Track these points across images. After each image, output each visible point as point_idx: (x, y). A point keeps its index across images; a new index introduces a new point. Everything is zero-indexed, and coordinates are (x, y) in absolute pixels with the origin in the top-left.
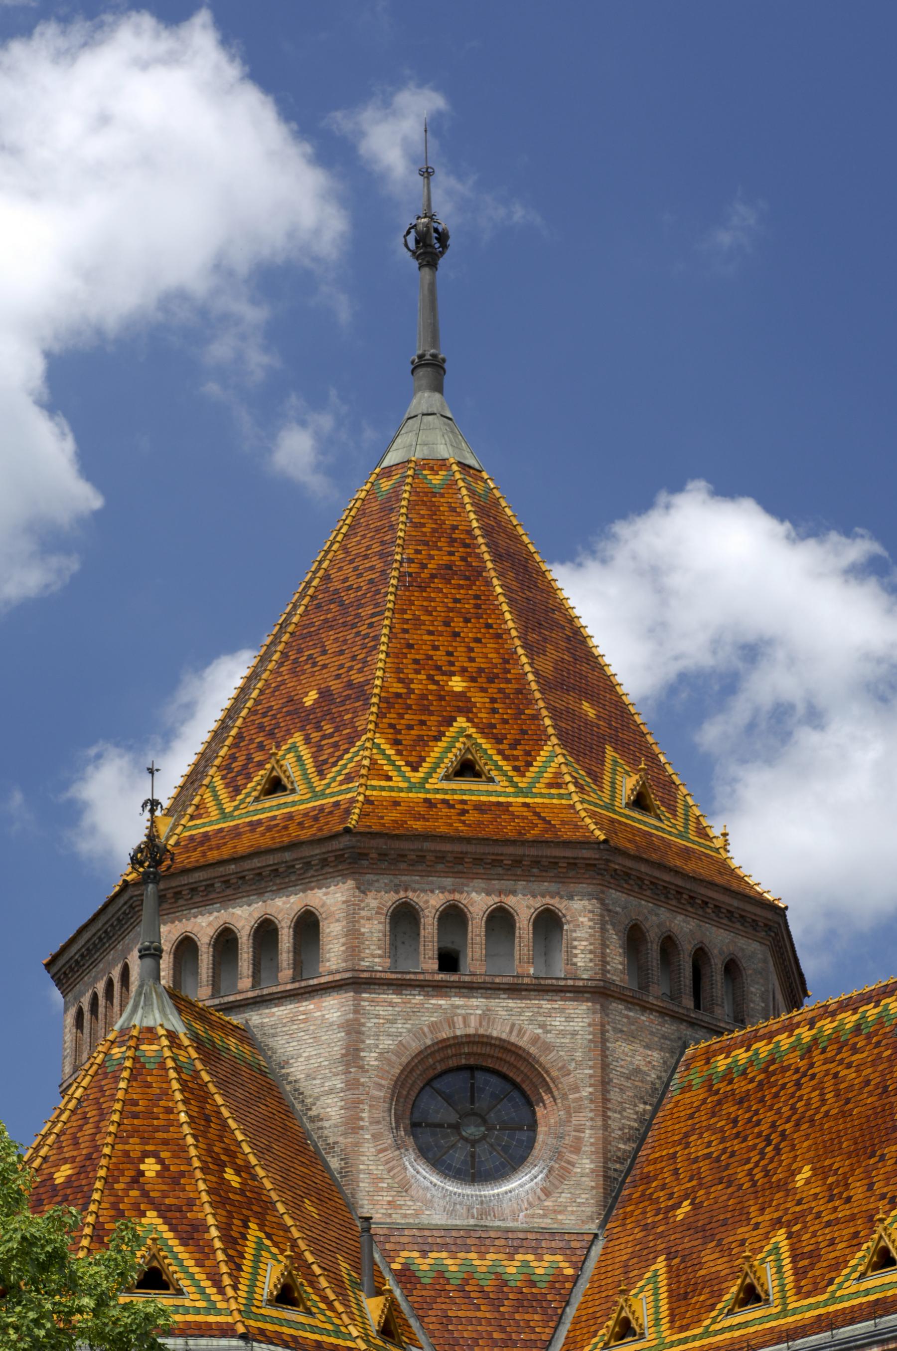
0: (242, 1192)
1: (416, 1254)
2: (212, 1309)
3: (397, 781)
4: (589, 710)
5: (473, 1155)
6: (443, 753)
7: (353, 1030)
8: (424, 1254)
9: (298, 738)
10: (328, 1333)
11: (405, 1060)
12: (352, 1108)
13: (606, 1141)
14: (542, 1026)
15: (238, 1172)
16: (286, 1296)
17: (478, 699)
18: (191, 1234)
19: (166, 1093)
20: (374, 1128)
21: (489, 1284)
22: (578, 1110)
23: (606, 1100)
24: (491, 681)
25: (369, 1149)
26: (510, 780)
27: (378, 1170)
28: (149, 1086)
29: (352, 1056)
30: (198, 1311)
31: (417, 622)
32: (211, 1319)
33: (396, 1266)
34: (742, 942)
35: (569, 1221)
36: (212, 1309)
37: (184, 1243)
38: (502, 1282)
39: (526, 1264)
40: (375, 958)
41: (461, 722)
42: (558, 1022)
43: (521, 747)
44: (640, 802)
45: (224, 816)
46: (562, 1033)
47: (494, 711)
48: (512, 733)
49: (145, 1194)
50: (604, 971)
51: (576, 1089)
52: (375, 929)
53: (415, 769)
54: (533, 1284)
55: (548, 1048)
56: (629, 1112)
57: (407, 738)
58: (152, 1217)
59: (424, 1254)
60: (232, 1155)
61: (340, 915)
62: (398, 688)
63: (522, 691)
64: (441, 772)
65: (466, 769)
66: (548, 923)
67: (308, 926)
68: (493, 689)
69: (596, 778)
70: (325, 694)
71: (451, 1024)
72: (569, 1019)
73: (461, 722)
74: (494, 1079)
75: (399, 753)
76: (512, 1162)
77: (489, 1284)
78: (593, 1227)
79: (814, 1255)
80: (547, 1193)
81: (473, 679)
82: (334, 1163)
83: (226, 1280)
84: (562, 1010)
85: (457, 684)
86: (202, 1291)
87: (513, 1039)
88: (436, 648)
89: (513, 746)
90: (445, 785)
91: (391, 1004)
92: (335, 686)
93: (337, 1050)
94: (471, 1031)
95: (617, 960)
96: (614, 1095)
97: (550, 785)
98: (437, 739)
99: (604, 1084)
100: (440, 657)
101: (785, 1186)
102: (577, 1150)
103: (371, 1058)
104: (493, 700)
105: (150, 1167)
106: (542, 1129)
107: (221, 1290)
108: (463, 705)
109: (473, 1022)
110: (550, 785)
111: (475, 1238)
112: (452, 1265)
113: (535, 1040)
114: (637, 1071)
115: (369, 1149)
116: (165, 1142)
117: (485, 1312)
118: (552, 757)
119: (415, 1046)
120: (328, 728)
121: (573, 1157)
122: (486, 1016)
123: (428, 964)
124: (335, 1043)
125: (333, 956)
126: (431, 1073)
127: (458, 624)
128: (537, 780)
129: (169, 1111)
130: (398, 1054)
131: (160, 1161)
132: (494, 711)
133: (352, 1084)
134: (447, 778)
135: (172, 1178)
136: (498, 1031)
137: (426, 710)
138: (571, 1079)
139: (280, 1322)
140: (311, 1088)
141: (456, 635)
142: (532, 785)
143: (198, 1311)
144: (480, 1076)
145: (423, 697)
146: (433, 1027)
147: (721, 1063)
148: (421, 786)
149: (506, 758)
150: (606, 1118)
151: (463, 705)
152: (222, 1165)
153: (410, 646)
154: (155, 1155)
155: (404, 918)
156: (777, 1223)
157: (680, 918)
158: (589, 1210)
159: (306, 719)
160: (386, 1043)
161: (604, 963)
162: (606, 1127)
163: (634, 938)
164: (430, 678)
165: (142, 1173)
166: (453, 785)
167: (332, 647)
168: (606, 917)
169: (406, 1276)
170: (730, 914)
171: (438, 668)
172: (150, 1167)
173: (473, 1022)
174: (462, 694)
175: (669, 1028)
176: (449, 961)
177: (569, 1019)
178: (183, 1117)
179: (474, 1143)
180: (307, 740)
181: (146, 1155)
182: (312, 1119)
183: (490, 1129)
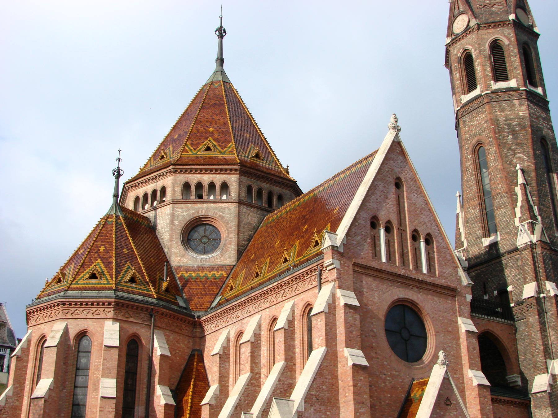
0: (127, 254)
1: (184, 273)
2: (109, 283)
3: (190, 153)
4: (247, 135)
5: (204, 247)
6: (203, 146)
7: (173, 215)
8: (187, 272)
9: (171, 146)
10: (144, 290)
11: (185, 222)
12: (171, 236)
13: (238, 241)
14: (222, 212)
15: (127, 250)
16: (132, 280)
17: (216, 133)
18: (108, 264)
19: (112, 230)
20: (176, 240)
21: (203, 280)
22: (231, 233)
23: (239, 230)
24: (220, 128)
25: (174, 246)
26: (220, 152)
27: (177, 251)
28: (107, 228)
29: (172, 222)
30: (104, 284)
31: (204, 117)
32: (107, 286)
33: (179, 276)
34: (284, 190)
35: (227, 263)
36: (109, 283)
37: (106, 267)
38: (207, 278)
39: (214, 274)
40: (179, 197)
41: (210, 138)
42: (226, 211)
43: (224, 143)
44: (257, 156)
45: (151, 166)
46: (227, 214)
47: (219, 135)
48: (223, 140)
49: (99, 255)
50: (239, 197)
51: (230, 228)
52: (179, 189)
53: (195, 150)
54: (215, 279)
55: (223, 217)
56: (246, 234)
57: (195, 143)
58: (99, 261)
59: (187, 272)
60: (127, 245)
61: (170, 186)
62: (196, 132)
63: (228, 131)
64: (202, 150)
65: (208, 149)
66: (225, 186)
67: (163, 190)
68: (220, 131)
69: (245, 151)
70: (179, 135)
71: (198, 213)
72: (229, 210)
73: (210, 138)
74: (211, 227)
75: (192, 146)
76: (215, 248)
77: (203, 280)
78: (234, 264)
79: (273, 263)
80: (222, 256)
81: (215, 129)
82: (166, 250)
83: (114, 276)
84: (228, 207)
85: (211, 130)
86: (107, 279)
87: (214, 215)
88: (207, 122)
89: (222, 143)
90: (202, 153)
91: (182, 208)
92: (182, 133)
93: (168, 221)
94: (203, 214)
95: (244, 194)
96: (242, 229)
97: (230, 152)
98: (203, 142)
99: (239, 226)
100: (208, 124)
101: (273, 247)
102: (230, 244)
103: (176, 222)
104: (219, 133)
105: (102, 249)
106: (222, 239)
107: (112, 278)
108: (212, 135)
109: (204, 212)
110: (230, 152)
111: (201, 268)
112: (194, 275)
113: (220, 216)
114: (249, 223)
115: (174, 246)
116: (108, 242)
117: (201, 287)
118: (232, 145)
119: (188, 219)
120: (177, 142)
121: (229, 246)
122: (208, 210)
123: (193, 197)
124: (168, 218)
125: (168, 197)
126: (194, 226)
127: (214, 116)
128: (227, 151)
129: (111, 234)
130: (183, 221)
131: (105, 247)
132: (219, 135)
133: (171, 229)
134: (203, 151)
135: (106, 251)
136: (210, 214)
137: (202, 136)
138: (229, 225)
139: (128, 287)
140: (162, 231)
141: (213, 119)
142: (225, 152)
143: (104, 284)
144: (207, 226)
145: (202, 133)
146: (193, 213)
147: (271, 219)
148: (196, 154)
149: (220, 146)
150: (238, 235)
151: (212, 135)
152: (123, 248)
153: (201, 122)
154: (104, 245)
155: (186, 186)
156: (269, 256)
157: (264, 184)
158: (233, 260)
159: (174, 141)
160: (181, 218)
161: (239, 195)
162: (238, 237)
163: (249, 190)
164: (205, 129)
165: (99, 250)
166: (204, 153)
167: (184, 124)
168: (240, 183)
169: (181, 278)
170: (279, 183)
171: (207, 126)
172: (102, 249)
173: (204, 212)
174: (212, 133)
175: (260, 212)
176: (200, 197)
177: (229, 210)
178: (114, 236)
179: (205, 244)
180: (172, 147)
181: (102, 245)
182: (162, 239)
183: (209, 240)
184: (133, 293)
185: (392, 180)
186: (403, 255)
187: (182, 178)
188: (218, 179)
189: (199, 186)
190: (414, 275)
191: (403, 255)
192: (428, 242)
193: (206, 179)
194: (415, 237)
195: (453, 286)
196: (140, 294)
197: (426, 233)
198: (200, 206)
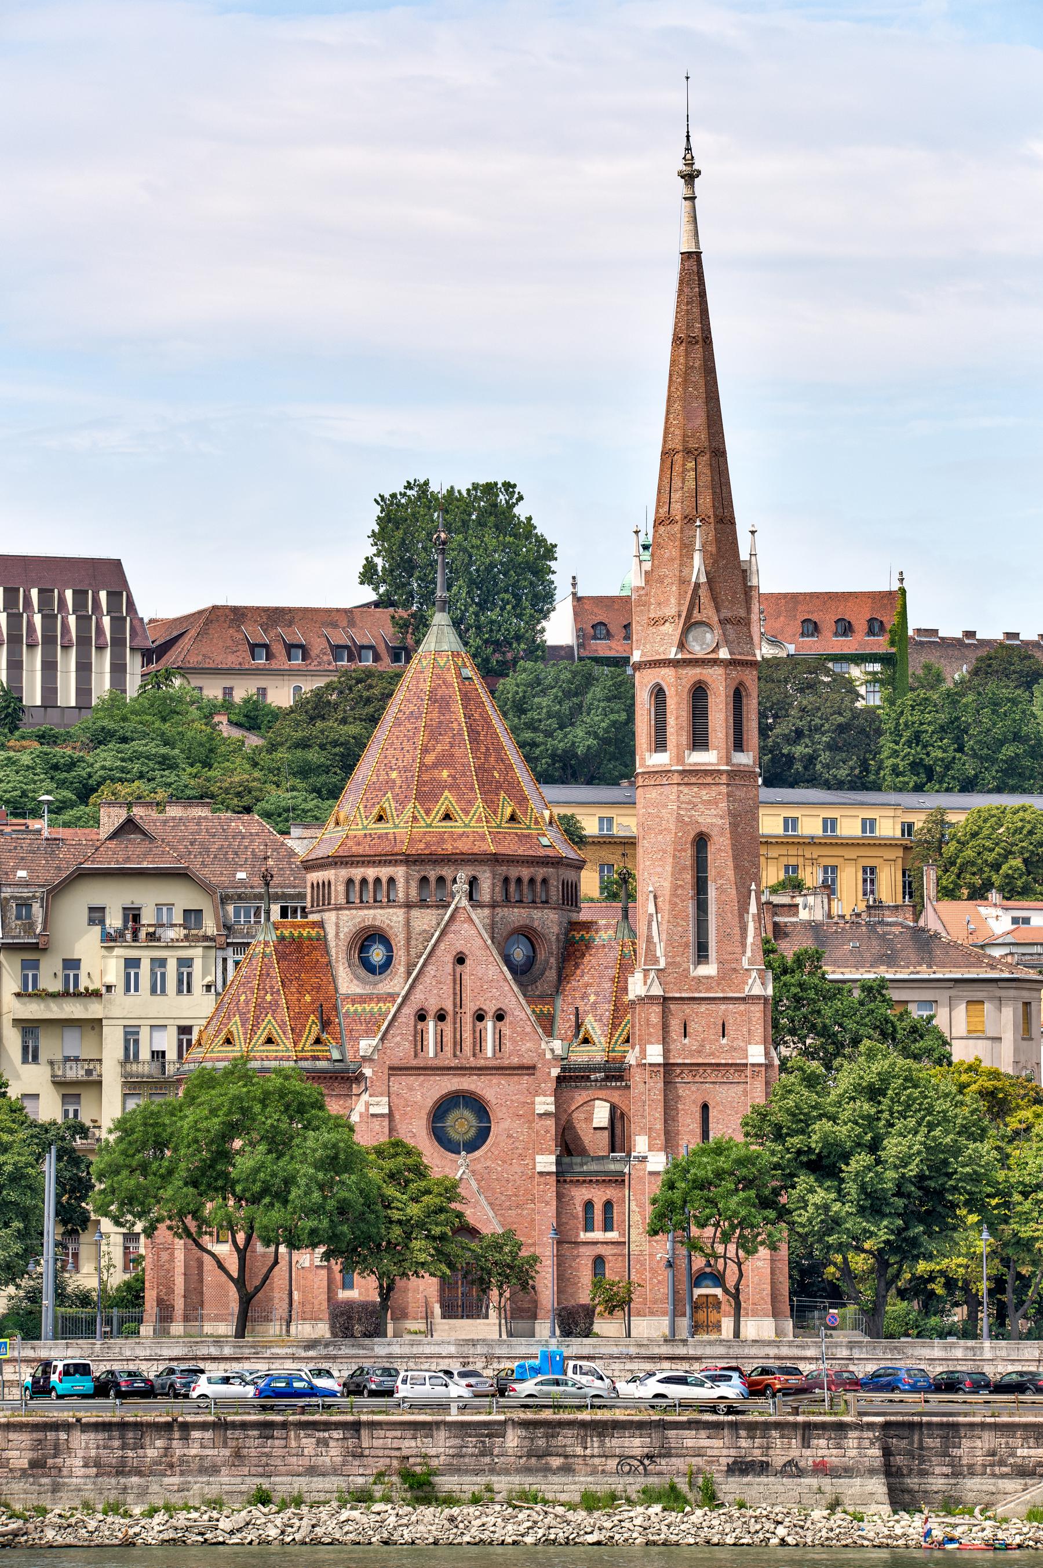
17: (398, 782)
25: (341, 968)
27: (344, 975)
40: (342, 900)
52: (341, 888)
55: (391, 928)
58: (237, 1018)
66: (391, 880)
69: (428, 812)
73: (389, 795)
85: (394, 775)
96: (413, 942)
103: (342, 936)
122: (374, 919)
135: (247, 1002)
148: (365, 828)
160: (346, 930)
184: (268, 1058)
185: (449, 959)
186: (458, 1044)
187: (344, 873)
188: (384, 872)
189: (364, 881)
190: (473, 1062)
191: (458, 1044)
192: (500, 1017)
193: (371, 873)
194: (480, 1017)
195: (526, 1061)
196: (276, 1059)
197: (494, 1009)
198: (366, 912)
